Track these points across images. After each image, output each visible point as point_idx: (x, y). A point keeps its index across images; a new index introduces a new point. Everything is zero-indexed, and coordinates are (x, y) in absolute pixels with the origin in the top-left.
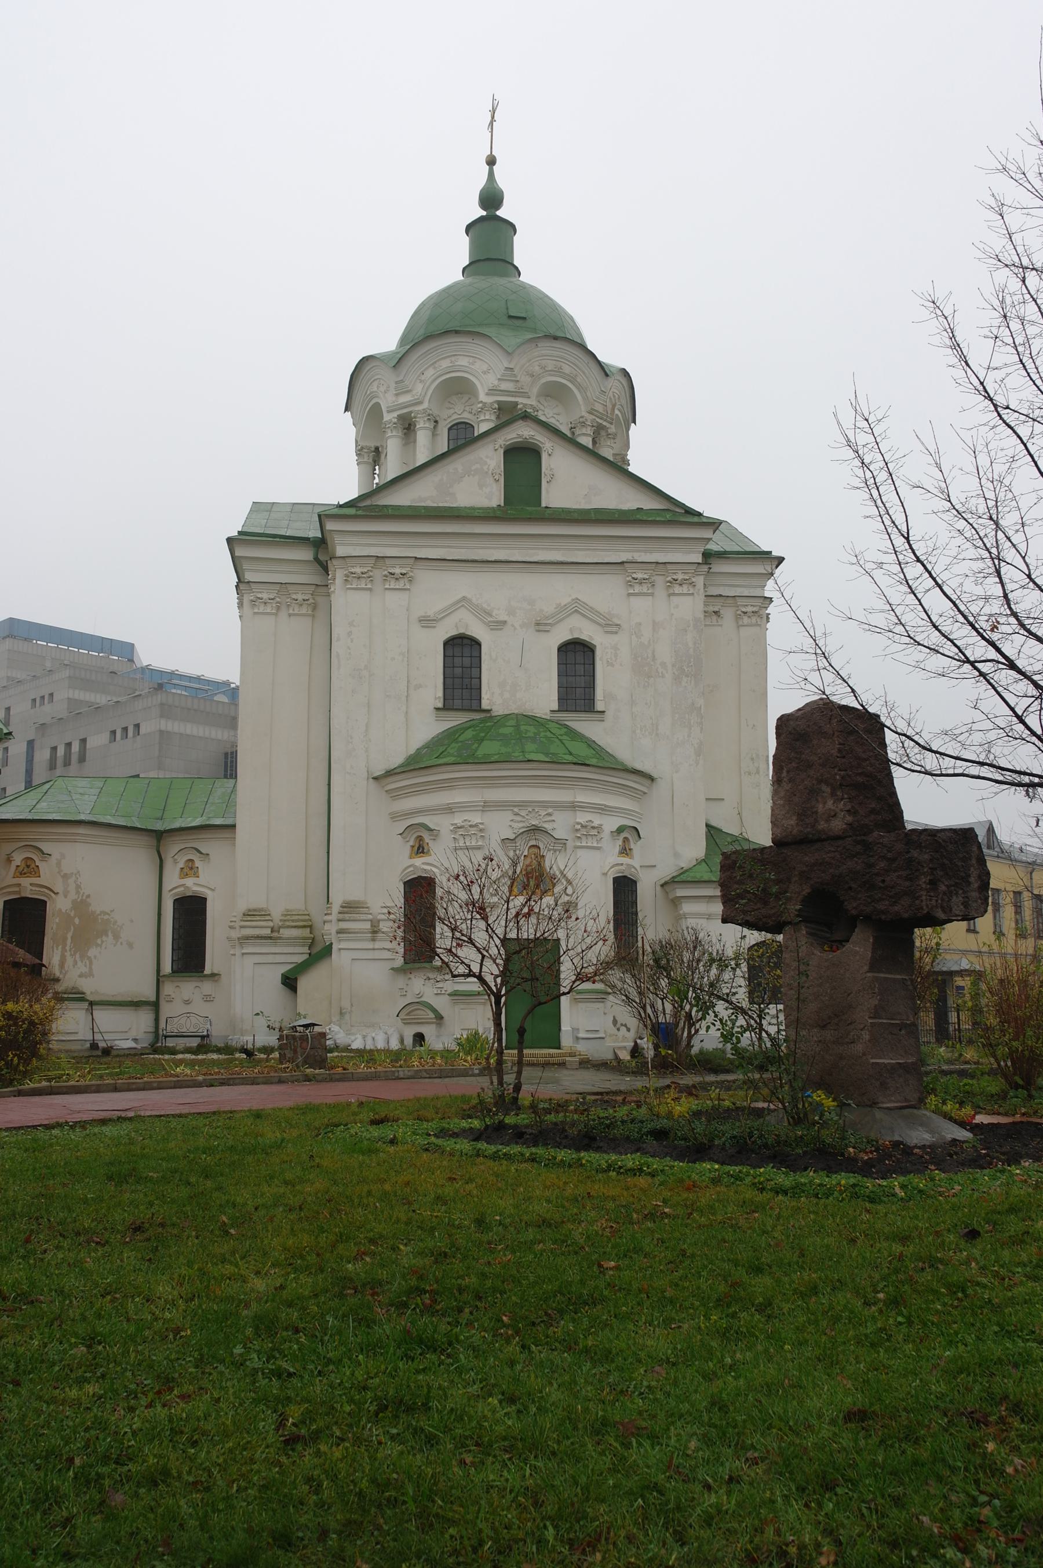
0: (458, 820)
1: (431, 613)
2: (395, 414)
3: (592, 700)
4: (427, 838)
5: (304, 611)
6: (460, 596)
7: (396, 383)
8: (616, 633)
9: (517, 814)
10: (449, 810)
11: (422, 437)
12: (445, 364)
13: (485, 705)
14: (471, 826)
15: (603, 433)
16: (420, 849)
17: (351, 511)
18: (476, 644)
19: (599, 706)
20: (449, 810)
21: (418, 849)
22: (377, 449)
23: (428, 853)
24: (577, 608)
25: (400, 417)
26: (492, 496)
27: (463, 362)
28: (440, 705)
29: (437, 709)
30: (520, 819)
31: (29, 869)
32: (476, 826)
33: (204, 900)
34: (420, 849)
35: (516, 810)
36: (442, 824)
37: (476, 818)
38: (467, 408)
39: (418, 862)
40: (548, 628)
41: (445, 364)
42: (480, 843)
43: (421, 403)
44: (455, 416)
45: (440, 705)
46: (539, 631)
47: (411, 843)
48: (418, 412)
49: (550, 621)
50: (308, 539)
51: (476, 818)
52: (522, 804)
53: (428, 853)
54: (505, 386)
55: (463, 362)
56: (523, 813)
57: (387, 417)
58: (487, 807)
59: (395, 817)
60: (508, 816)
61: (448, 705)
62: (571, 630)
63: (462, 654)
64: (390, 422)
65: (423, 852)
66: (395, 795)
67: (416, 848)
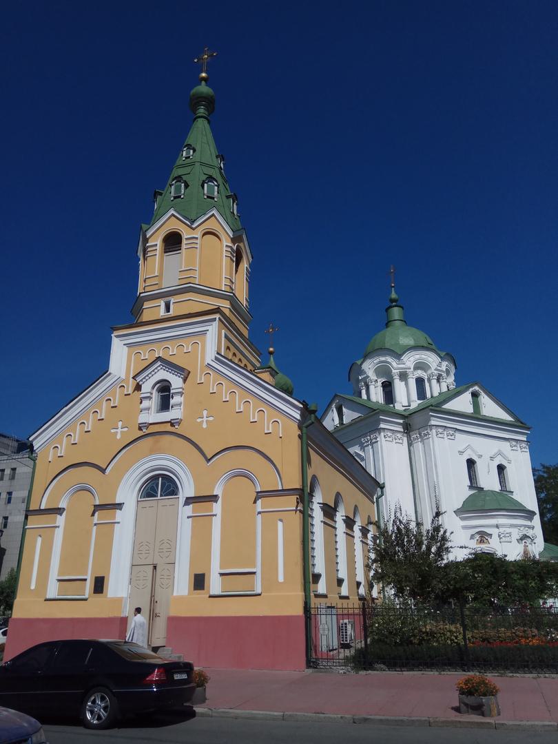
0: (501, 530)
1: (461, 450)
6: (467, 445)
10: (497, 526)
12: (418, 356)
20: (497, 526)
24: (500, 453)
26: (469, 409)
32: (510, 533)
34: (482, 541)
36: (494, 531)
37: (508, 530)
41: (418, 356)
47: (477, 538)
51: (508, 530)
52: (521, 526)
55: (423, 356)
59: (465, 527)
62: (500, 461)
66: (463, 519)
67: (479, 541)
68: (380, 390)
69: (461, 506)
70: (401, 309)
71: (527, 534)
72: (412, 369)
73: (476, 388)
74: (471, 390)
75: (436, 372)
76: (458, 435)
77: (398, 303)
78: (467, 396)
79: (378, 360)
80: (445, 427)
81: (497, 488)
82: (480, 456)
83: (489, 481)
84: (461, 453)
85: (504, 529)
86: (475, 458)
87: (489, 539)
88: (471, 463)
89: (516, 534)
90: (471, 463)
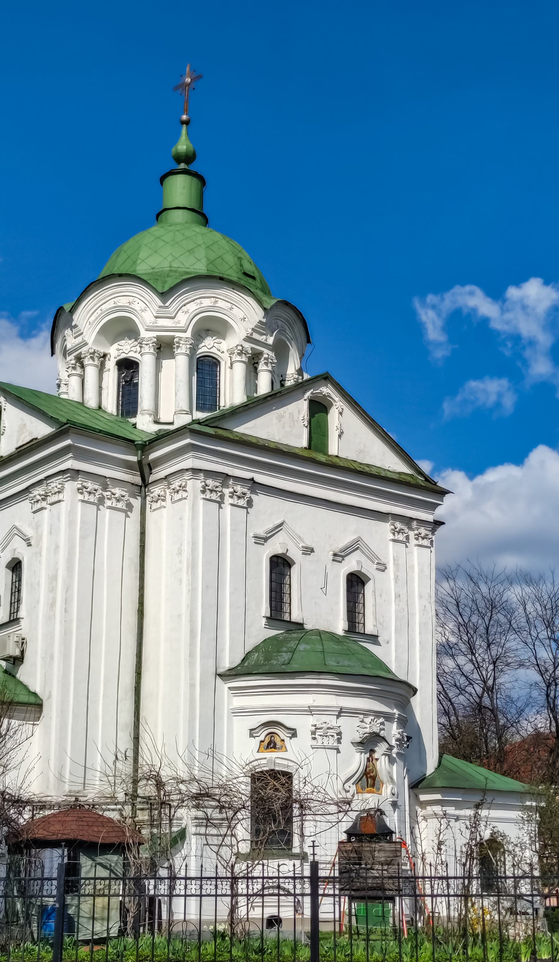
1: (261, 532)
2: (155, 334)
4: (282, 734)
5: (120, 505)
7: (160, 307)
8: (383, 571)
9: (362, 721)
10: (310, 711)
12: (207, 303)
14: (329, 728)
17: (211, 431)
21: (269, 744)
22: (105, 356)
23: (283, 748)
25: (158, 337)
27: (221, 304)
29: (267, 618)
30: (363, 725)
34: (271, 745)
35: (361, 716)
37: (332, 721)
38: (216, 345)
40: (340, 559)
41: (207, 303)
42: (335, 744)
43: (185, 331)
44: (214, 350)
45: (269, 615)
46: (333, 560)
47: (262, 738)
48: (180, 338)
49: (342, 554)
50: (133, 441)
51: (332, 721)
52: (366, 713)
53: (283, 748)
54: (256, 336)
55: (221, 304)
56: (368, 720)
57: (144, 334)
58: (341, 712)
60: (355, 721)
64: (150, 339)
65: (275, 747)
68: (111, 376)
69: (238, 661)
70: (195, 180)
71: (382, 733)
72: (189, 334)
73: (327, 390)
74: (308, 394)
75: (248, 346)
76: (260, 499)
77: (193, 167)
78: (300, 408)
79: (110, 304)
80: (227, 476)
81: (340, 626)
82: (308, 551)
83: (319, 606)
84: (261, 540)
85: (324, 718)
86: (295, 554)
87: (287, 740)
88: (280, 565)
90: (280, 565)
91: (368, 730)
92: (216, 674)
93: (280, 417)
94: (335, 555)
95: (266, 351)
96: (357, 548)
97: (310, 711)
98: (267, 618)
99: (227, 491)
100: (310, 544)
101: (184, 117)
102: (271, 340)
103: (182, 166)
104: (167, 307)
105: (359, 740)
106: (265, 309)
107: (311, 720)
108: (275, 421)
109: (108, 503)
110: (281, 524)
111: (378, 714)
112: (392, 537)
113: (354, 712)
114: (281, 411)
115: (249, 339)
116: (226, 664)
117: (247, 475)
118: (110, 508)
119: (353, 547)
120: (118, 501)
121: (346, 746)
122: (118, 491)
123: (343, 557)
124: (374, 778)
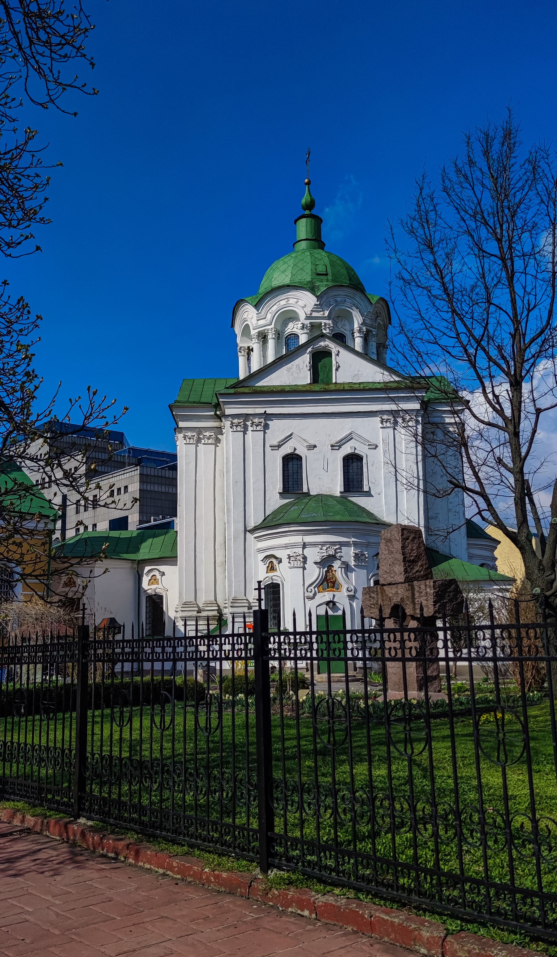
1: (275, 443)
2: (257, 331)
3: (362, 487)
5: (210, 441)
8: (375, 449)
10: (286, 547)
11: (271, 343)
12: (283, 303)
13: (305, 490)
15: (370, 334)
16: (272, 568)
18: (299, 458)
19: (366, 489)
28: (281, 491)
29: (280, 493)
30: (322, 551)
31: (70, 583)
33: (161, 597)
36: (282, 554)
39: (271, 574)
41: (283, 303)
45: (281, 491)
52: (323, 544)
56: (325, 548)
60: (317, 549)
61: (286, 491)
63: (292, 464)
69: (261, 521)
74: (310, 349)
75: (307, 322)
77: (314, 212)
78: (305, 360)
85: (294, 550)
86: (301, 451)
89: (314, 555)
91: (325, 554)
92: (246, 530)
93: (288, 370)
94: (332, 446)
95: (323, 321)
96: (352, 438)
97: (286, 547)
98: (280, 493)
99: (249, 423)
100: (313, 443)
101: (306, 180)
102: (327, 313)
103: (307, 212)
104: (260, 313)
105: (319, 561)
106: (317, 297)
107: (288, 552)
108: (285, 372)
109: (203, 441)
110: (291, 435)
111: (333, 543)
112: (381, 425)
113: (314, 544)
114: (289, 365)
115: (307, 318)
116: (251, 524)
117: (262, 411)
118: (204, 444)
119: (348, 438)
120: (209, 439)
121: (310, 564)
122: (208, 434)
123: (340, 447)
124: (334, 583)
